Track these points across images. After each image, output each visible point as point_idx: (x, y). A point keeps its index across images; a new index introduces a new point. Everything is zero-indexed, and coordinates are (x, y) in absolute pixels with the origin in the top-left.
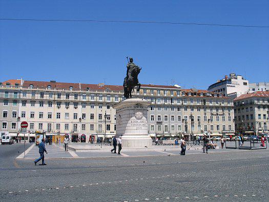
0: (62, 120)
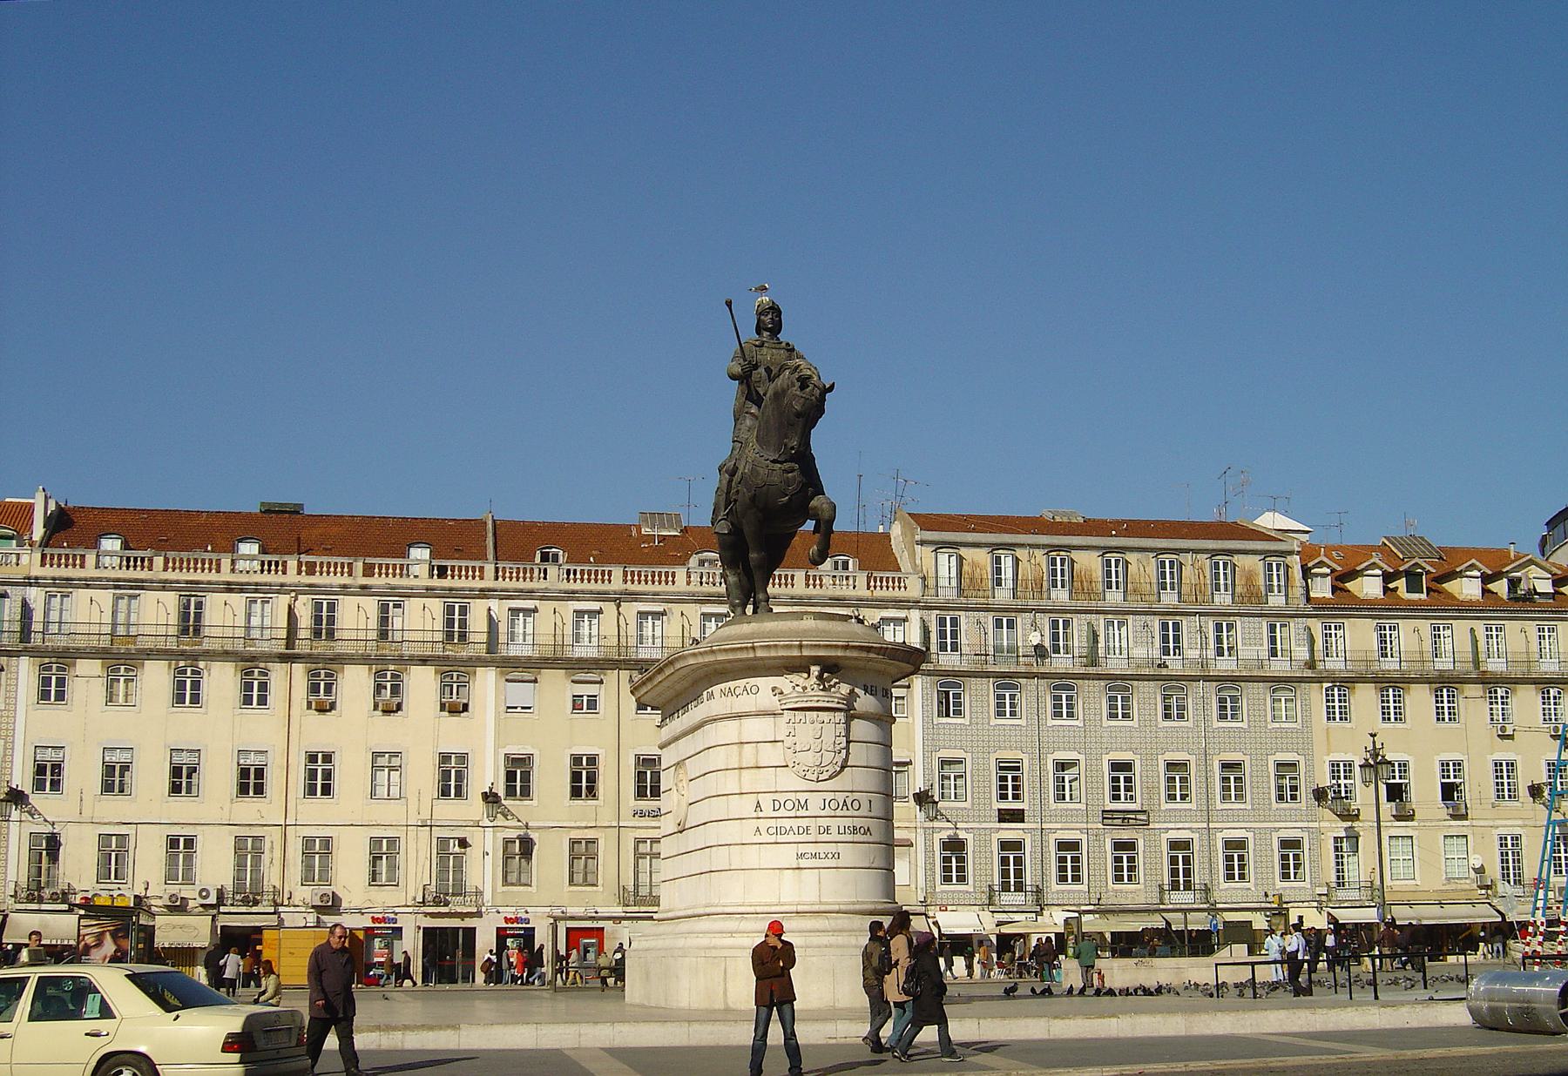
0: (349, 815)
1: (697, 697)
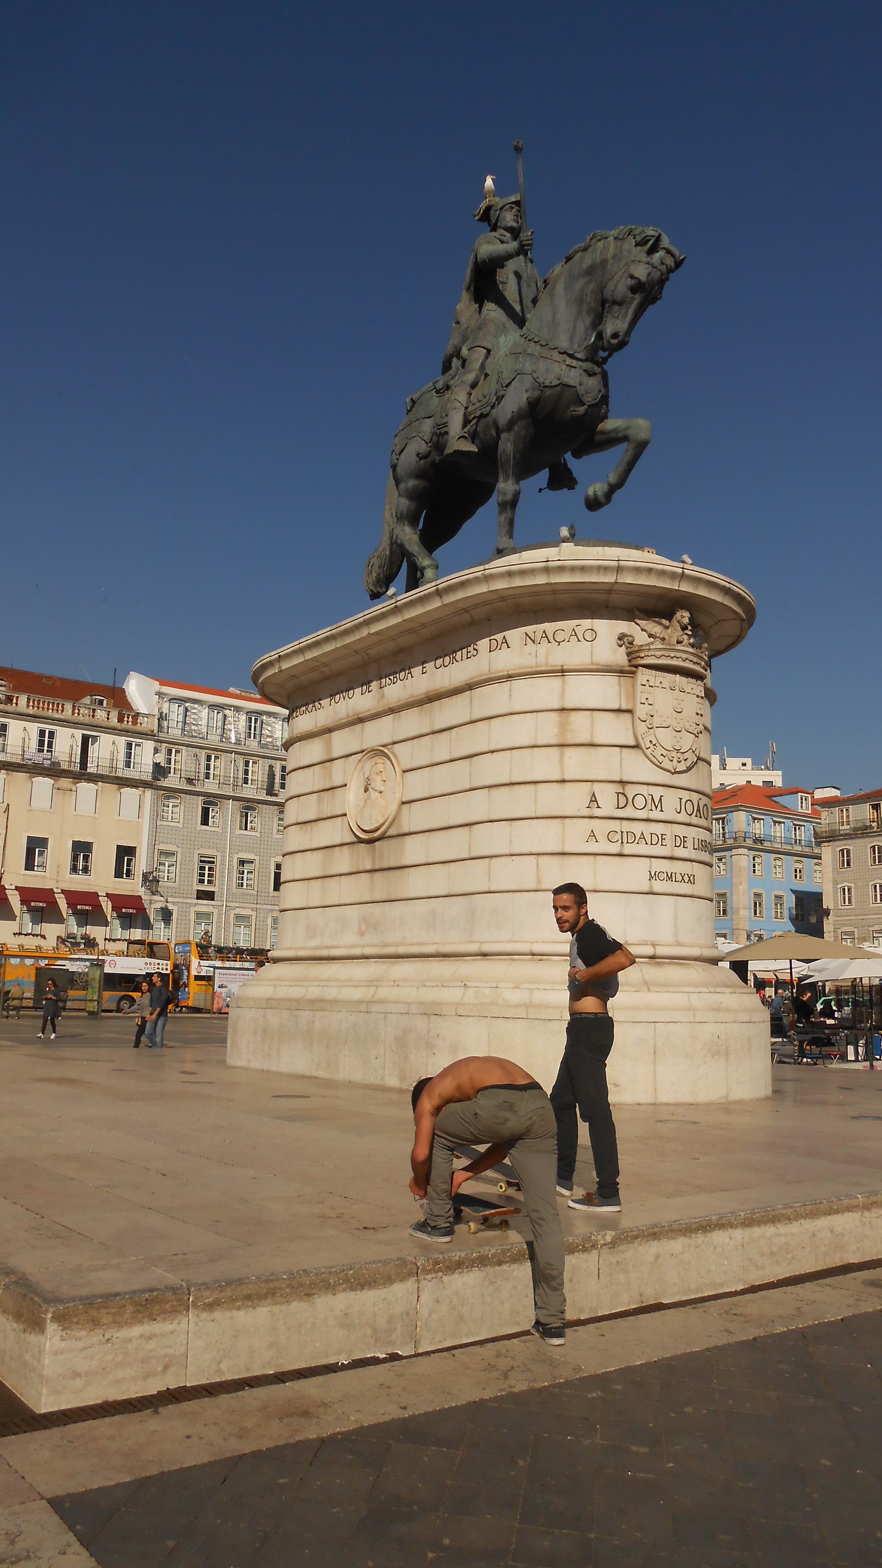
1: (407, 668)
